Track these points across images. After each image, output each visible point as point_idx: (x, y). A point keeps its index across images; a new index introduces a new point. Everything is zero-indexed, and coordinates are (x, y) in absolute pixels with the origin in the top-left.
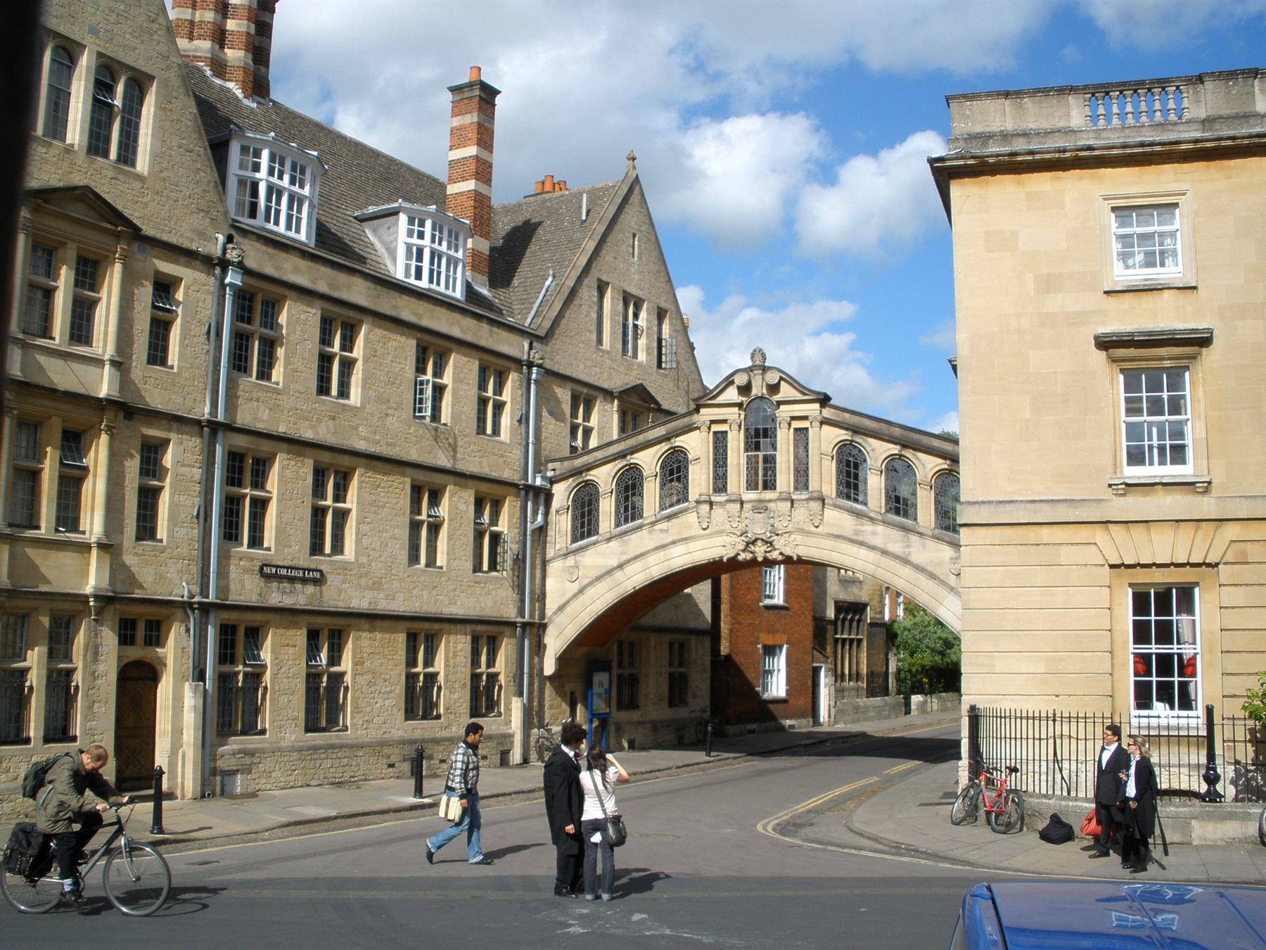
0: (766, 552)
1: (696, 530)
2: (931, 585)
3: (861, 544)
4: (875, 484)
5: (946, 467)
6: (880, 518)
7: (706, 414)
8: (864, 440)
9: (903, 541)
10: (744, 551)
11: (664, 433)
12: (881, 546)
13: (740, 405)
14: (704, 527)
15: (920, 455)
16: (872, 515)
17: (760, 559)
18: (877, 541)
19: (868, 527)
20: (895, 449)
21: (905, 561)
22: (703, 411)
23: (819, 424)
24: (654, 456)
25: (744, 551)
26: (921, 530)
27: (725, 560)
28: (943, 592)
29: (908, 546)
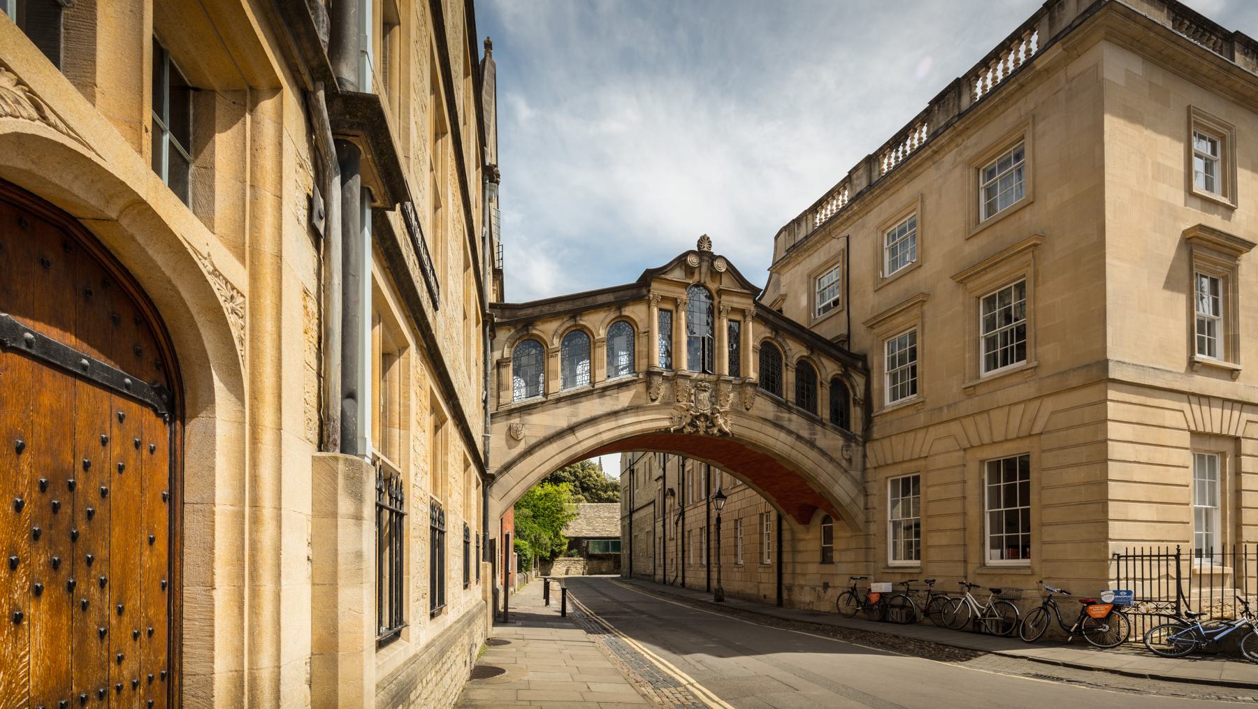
0: (707, 427)
1: (643, 401)
2: (830, 467)
3: (781, 428)
4: (789, 377)
5: (840, 372)
6: (795, 407)
7: (657, 289)
8: (784, 340)
9: (810, 429)
10: (689, 425)
11: (613, 300)
12: (796, 431)
13: (686, 286)
14: (654, 398)
15: (825, 361)
16: (790, 404)
17: (702, 433)
18: (793, 427)
19: (786, 415)
20: (805, 352)
21: (811, 444)
22: (654, 285)
23: (749, 319)
24: (602, 322)
25: (689, 425)
26: (824, 421)
27: (672, 429)
28: (838, 473)
29: (814, 434)
